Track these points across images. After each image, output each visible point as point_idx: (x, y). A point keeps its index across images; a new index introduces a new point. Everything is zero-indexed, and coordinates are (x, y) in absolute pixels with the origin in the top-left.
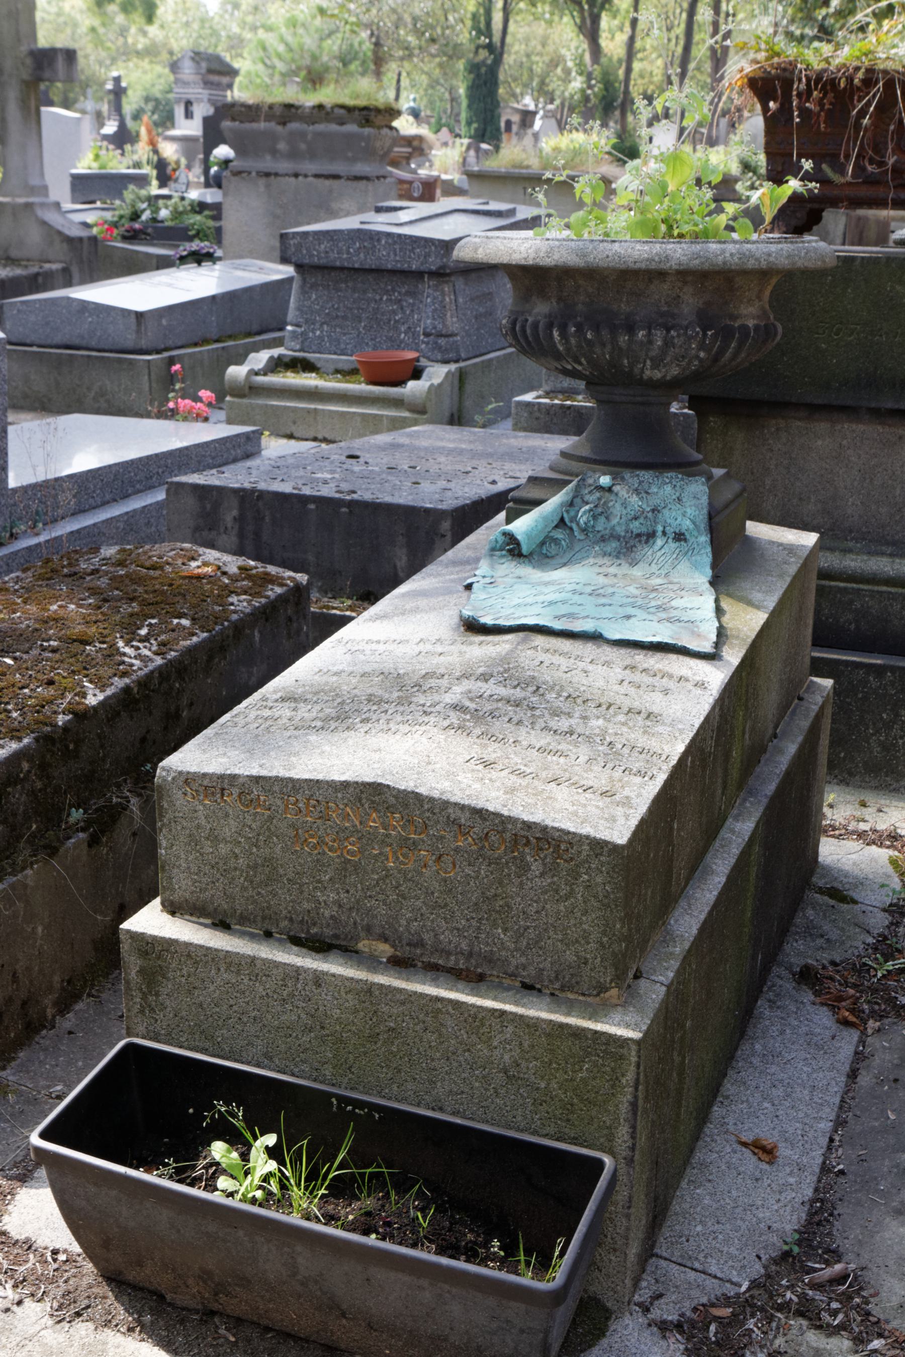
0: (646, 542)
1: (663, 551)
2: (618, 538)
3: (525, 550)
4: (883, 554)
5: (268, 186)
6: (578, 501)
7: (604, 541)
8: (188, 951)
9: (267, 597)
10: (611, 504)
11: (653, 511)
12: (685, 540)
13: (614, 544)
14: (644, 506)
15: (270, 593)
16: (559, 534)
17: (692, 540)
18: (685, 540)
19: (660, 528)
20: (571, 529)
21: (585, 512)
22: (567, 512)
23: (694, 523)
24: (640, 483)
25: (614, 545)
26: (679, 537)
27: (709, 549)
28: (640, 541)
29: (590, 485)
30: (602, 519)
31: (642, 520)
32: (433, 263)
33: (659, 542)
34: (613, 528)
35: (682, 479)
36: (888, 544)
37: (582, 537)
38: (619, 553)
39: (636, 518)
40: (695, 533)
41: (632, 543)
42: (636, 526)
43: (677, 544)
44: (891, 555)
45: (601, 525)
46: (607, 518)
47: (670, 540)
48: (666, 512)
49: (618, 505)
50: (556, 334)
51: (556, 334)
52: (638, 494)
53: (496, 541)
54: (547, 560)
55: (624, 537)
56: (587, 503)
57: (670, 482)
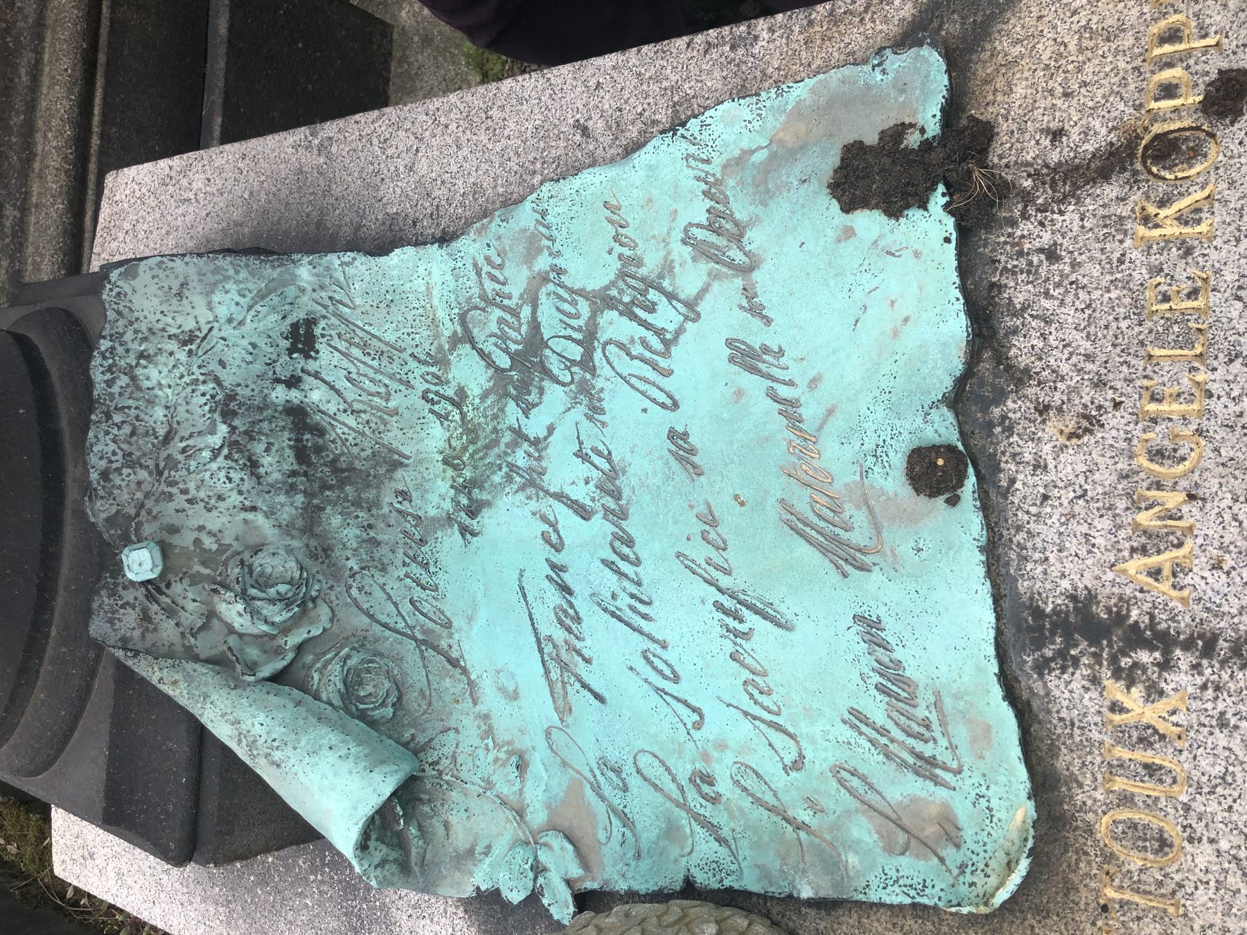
0: (320, 431)
1: (342, 384)
6: (203, 645)
7: (327, 551)
10: (209, 543)
12: (310, 322)
13: (333, 520)
14: (216, 440)
16: (329, 679)
18: (310, 322)
19: (280, 394)
20: (300, 648)
21: (254, 613)
22: (252, 668)
24: (131, 462)
25: (336, 521)
26: (302, 338)
27: (333, 259)
28: (318, 450)
29: (146, 617)
30: (265, 563)
31: (259, 448)
33: (317, 395)
35: (117, 337)
37: (324, 611)
38: (357, 504)
39: (253, 465)
40: (291, 291)
41: (323, 472)
43: (322, 346)
44: (24, 209)
45: (279, 563)
46: (257, 549)
47: (312, 366)
49: (214, 521)
52: (172, 463)
53: (382, 863)
54: (412, 698)
55: (309, 494)
56: (211, 615)
57: (130, 372)
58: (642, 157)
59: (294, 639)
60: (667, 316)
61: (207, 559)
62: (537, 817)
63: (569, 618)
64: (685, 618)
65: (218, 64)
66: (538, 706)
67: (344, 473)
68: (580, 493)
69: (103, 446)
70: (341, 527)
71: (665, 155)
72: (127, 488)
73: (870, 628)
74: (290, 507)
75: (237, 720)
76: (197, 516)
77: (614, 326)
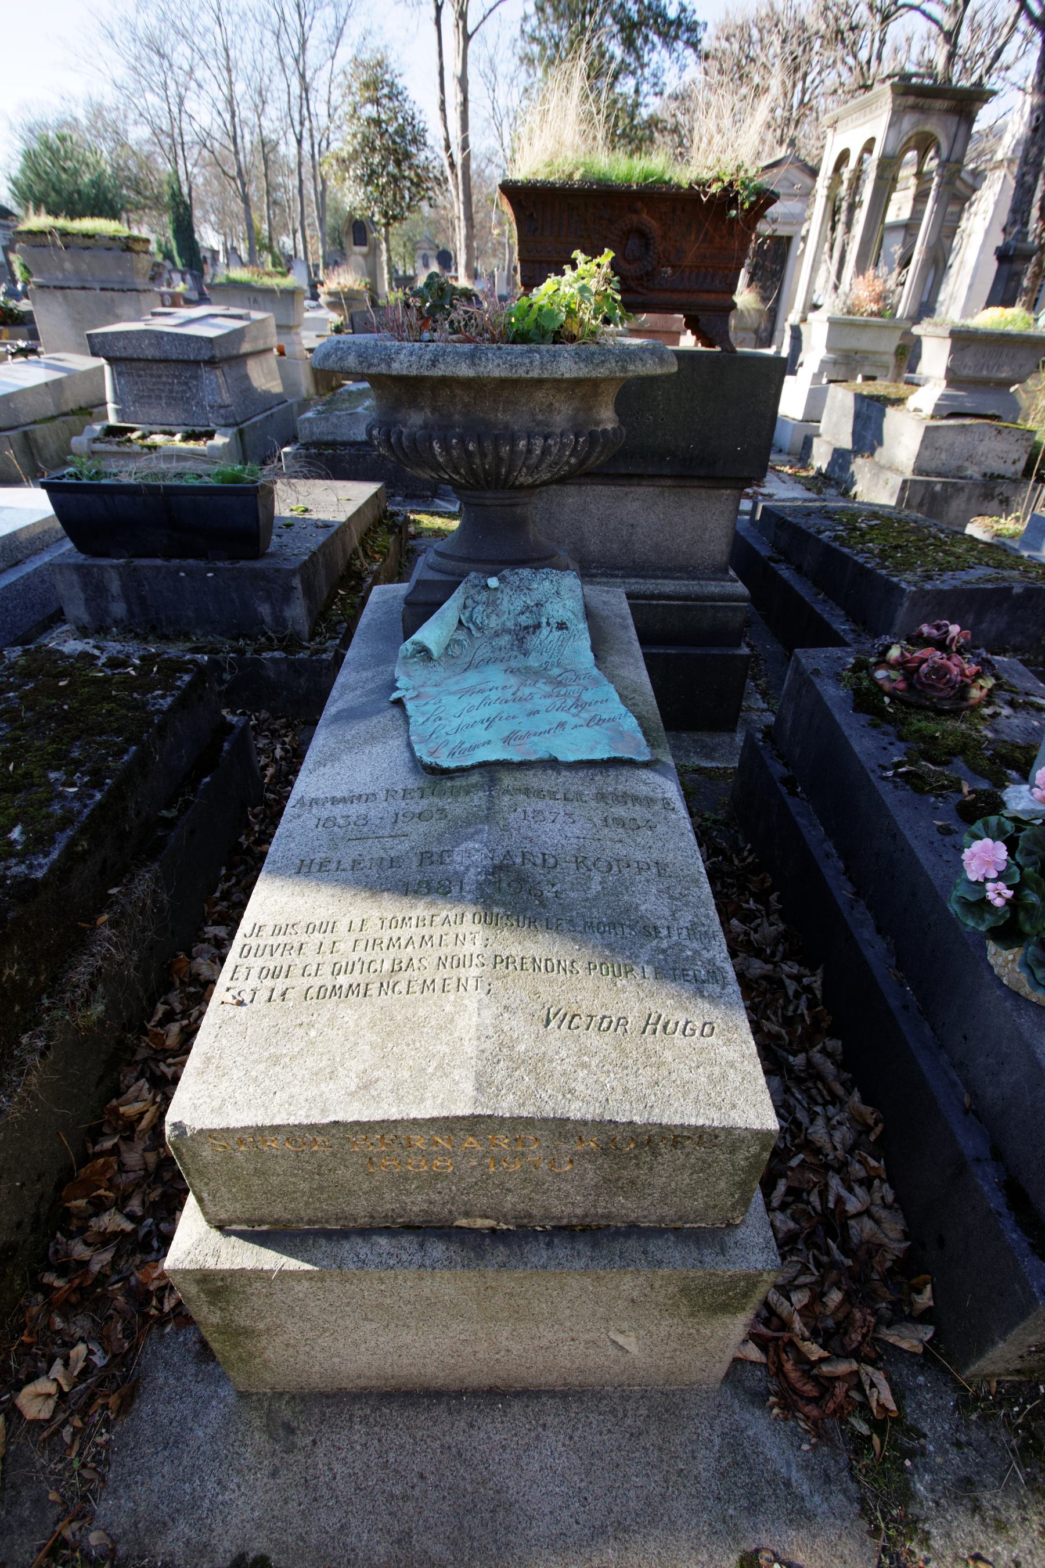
2: (509, 632)
3: (435, 654)
4: (617, 576)
5: (65, 297)
8: (259, 1275)
9: (179, 688)
11: (537, 605)
15: (179, 683)
17: (572, 628)
19: (544, 620)
20: (469, 629)
23: (573, 613)
24: (521, 580)
26: (562, 626)
27: (587, 635)
30: (494, 617)
32: (205, 355)
33: (545, 631)
34: (503, 624)
36: (618, 569)
39: (523, 613)
41: (521, 635)
42: (524, 620)
48: (548, 605)
49: (505, 602)
50: (436, 446)
51: (436, 446)
58: (622, 707)
59: (471, 626)
60: (573, 710)
61: (494, 602)
62: (422, 690)
63: (481, 691)
64: (487, 712)
65: (698, 651)
66: (455, 688)
67: (521, 641)
68: (519, 694)
69: (525, 572)
70: (505, 640)
71: (623, 709)
72: (514, 579)
73: (489, 742)
74: (510, 625)
75: (450, 610)
76: (506, 599)
77: (570, 702)
